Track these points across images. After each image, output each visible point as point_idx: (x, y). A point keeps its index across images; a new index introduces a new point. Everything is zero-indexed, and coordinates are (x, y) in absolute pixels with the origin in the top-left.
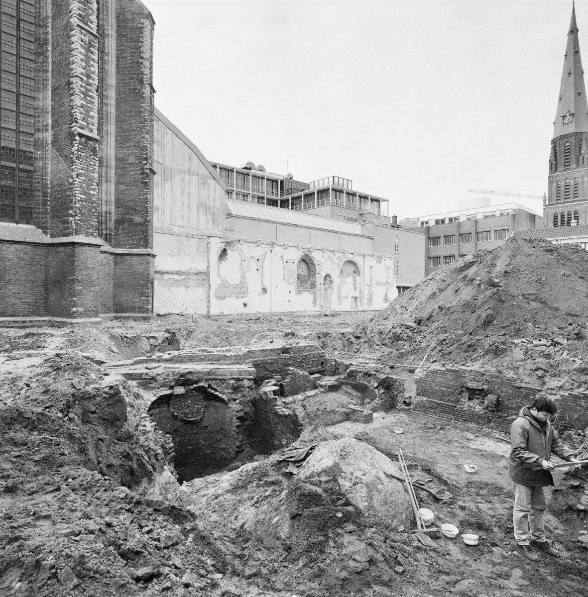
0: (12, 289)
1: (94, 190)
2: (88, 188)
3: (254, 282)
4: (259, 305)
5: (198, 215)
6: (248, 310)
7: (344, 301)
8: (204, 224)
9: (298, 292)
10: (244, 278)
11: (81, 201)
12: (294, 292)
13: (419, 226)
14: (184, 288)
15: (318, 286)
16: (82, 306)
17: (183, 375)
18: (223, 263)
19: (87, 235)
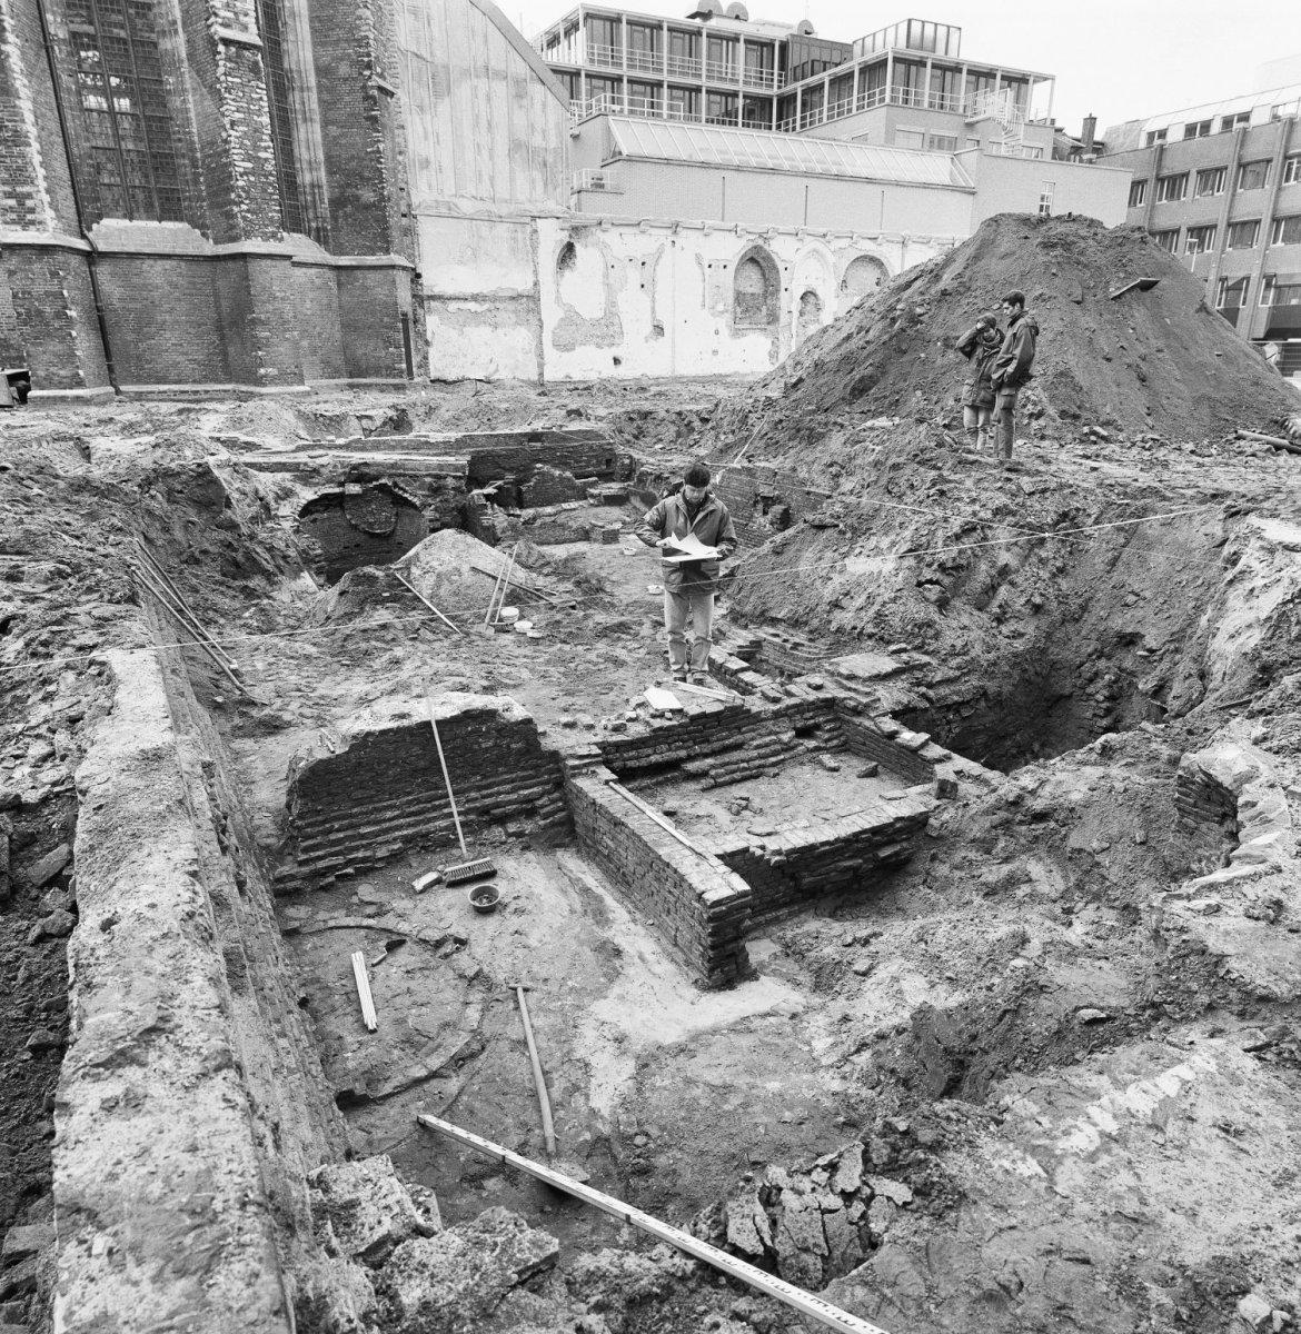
0: (170, 338)
1: (266, 149)
2: (256, 148)
3: (634, 312)
4: (645, 361)
5: (512, 171)
6: (623, 372)
8: (526, 189)
9: (736, 333)
10: (614, 304)
11: (246, 173)
12: (725, 332)
13: (1143, 143)
14: (488, 330)
15: (784, 318)
16: (273, 365)
17: (355, 467)
18: (567, 273)
19: (266, 237)
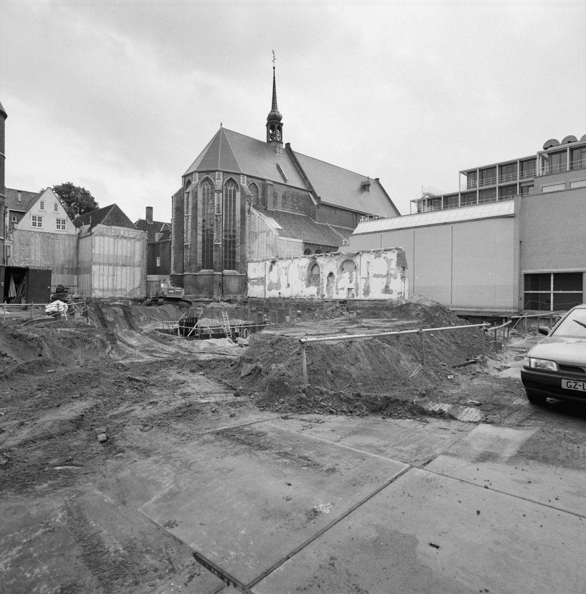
4: (286, 293)
7: (341, 292)
10: (280, 279)
12: (305, 286)
